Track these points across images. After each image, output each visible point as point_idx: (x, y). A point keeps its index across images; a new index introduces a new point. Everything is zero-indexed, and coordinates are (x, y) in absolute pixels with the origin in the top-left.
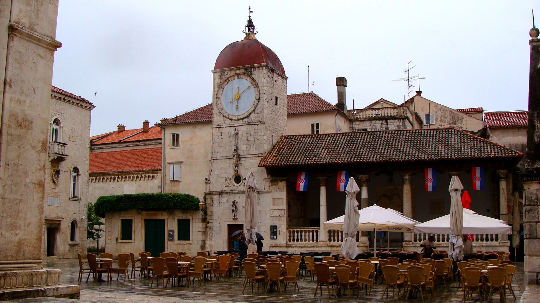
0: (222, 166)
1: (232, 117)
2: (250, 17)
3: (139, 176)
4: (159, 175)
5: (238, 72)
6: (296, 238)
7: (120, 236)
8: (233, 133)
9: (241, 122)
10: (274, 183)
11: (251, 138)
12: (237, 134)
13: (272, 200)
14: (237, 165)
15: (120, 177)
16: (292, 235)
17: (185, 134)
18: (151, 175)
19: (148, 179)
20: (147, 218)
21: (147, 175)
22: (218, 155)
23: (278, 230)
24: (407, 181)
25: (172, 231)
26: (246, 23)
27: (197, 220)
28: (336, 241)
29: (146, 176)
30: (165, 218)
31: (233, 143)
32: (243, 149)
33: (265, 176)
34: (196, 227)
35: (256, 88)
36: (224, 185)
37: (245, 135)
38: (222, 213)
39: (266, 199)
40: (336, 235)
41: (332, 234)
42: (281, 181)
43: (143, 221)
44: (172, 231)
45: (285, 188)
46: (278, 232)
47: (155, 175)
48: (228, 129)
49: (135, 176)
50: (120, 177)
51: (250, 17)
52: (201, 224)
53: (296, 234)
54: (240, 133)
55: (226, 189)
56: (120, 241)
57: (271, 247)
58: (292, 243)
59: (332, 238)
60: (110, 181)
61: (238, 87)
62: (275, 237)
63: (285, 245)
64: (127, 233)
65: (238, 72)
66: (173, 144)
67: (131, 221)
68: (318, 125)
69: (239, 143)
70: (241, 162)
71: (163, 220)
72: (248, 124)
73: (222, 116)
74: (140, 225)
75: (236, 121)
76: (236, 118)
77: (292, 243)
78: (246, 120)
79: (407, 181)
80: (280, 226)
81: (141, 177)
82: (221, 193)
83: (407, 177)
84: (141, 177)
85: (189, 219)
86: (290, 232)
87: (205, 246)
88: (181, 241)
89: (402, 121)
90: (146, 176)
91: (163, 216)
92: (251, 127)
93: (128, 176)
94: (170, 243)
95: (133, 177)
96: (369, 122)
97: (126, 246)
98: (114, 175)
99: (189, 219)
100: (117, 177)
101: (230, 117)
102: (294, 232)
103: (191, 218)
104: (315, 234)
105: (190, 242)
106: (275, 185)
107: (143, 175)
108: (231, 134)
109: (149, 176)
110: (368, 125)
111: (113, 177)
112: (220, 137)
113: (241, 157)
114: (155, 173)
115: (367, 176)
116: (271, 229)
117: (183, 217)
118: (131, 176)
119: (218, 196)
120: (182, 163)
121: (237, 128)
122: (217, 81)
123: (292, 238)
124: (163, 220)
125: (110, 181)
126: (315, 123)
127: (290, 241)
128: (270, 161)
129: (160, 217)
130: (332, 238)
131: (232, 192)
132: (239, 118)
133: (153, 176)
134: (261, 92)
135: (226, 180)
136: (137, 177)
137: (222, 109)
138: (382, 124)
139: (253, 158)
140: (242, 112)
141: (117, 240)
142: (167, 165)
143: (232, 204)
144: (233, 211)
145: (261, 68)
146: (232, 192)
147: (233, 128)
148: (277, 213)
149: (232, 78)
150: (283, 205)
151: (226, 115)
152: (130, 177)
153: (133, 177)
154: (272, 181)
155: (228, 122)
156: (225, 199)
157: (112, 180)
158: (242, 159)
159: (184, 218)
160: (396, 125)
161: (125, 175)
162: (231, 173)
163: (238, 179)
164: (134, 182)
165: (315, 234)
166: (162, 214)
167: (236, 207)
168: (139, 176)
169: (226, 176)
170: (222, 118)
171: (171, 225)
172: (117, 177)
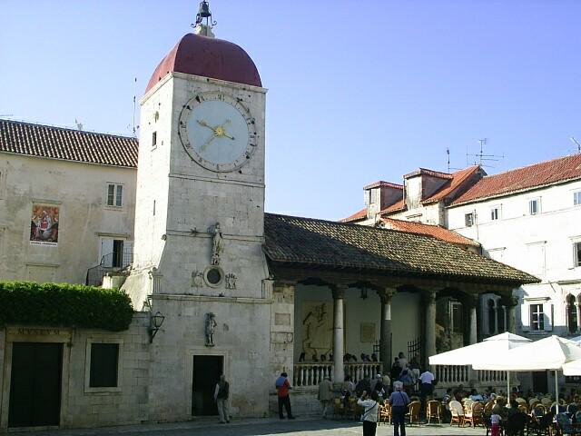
0: (186, 249)
10: (277, 289)
11: (242, 209)
16: (297, 374)
20: (21, 339)
24: (433, 301)
26: (198, 9)
30: (66, 340)
32: (228, 224)
33: (265, 272)
36: (190, 283)
38: (185, 336)
39: (265, 313)
42: (289, 286)
52: (140, 355)
54: (222, 195)
55: (193, 291)
57: (271, 394)
76: (214, 168)
77: (297, 387)
78: (234, 175)
79: (433, 301)
85: (117, 346)
87: (147, 396)
88: (100, 389)
91: (62, 337)
99: (117, 346)
102: (300, 368)
103: (121, 342)
106: (279, 291)
119: (176, 304)
122: (183, 96)
123: (297, 379)
124: (59, 347)
128: (281, 254)
129: (52, 338)
135: (194, 275)
137: (188, 146)
139: (245, 243)
143: (202, 318)
148: (281, 338)
151: (197, 159)
154: (274, 285)
155: (200, 171)
156: (189, 310)
162: (204, 266)
163: (215, 276)
166: (57, 333)
169: (194, 267)
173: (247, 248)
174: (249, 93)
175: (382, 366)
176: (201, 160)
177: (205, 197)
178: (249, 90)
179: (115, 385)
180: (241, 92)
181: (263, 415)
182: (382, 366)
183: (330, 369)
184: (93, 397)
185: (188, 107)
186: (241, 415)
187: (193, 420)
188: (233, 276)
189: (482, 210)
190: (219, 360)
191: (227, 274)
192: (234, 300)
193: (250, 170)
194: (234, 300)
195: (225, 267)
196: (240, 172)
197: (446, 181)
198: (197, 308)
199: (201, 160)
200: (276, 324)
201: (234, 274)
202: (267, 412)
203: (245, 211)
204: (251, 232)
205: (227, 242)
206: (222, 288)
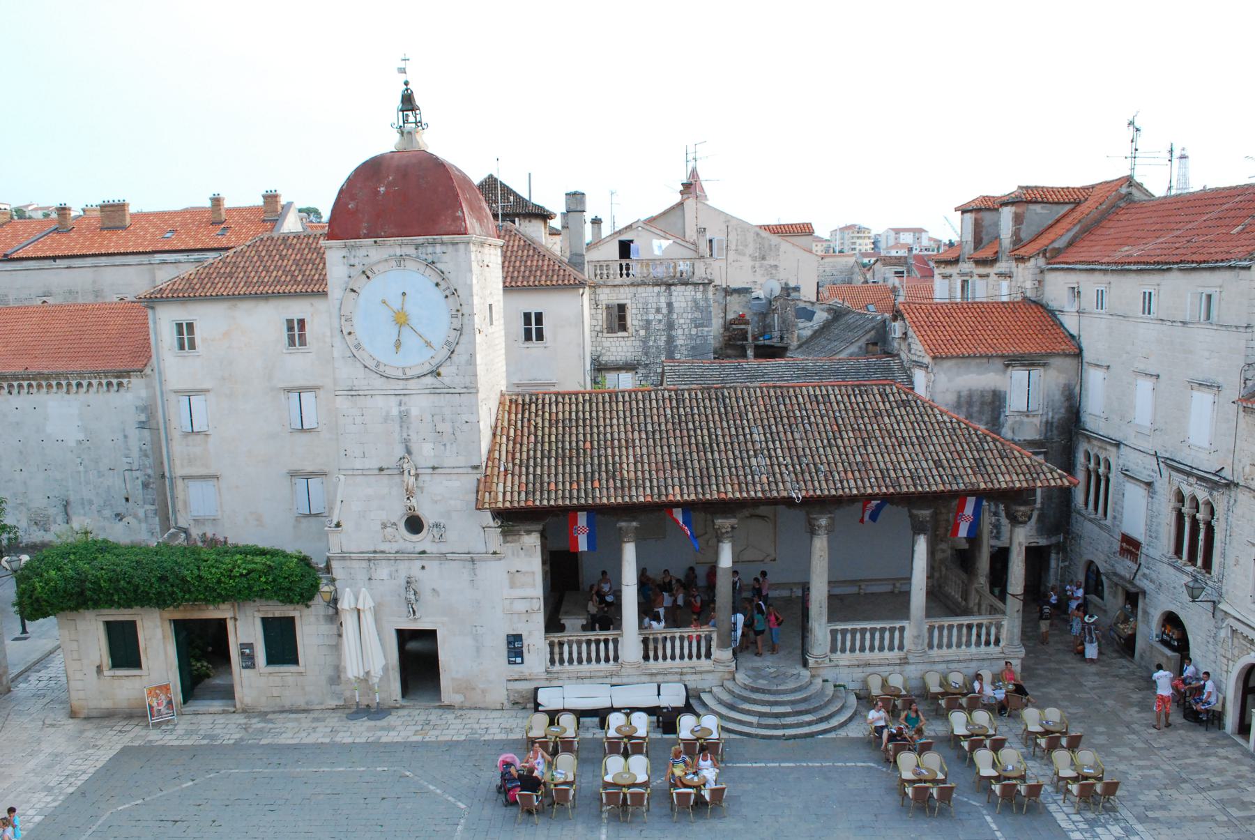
1: (389, 372)
2: (406, 83)
3: (85, 383)
4: (133, 380)
5: (398, 251)
6: (566, 656)
7: (107, 661)
8: (395, 411)
9: (412, 384)
10: (509, 538)
11: (445, 427)
12: (404, 417)
13: (505, 575)
14: (410, 494)
15: (34, 383)
17: (209, 320)
18: (115, 381)
19: (108, 390)
20: (179, 615)
21: (104, 382)
22: (358, 464)
23: (526, 643)
25: (250, 646)
27: (313, 619)
28: (660, 659)
29: (100, 384)
31: (396, 436)
32: (426, 452)
34: (310, 630)
35: (451, 299)
37: (428, 418)
39: (493, 573)
40: (660, 647)
41: (651, 646)
42: (529, 532)
43: (170, 631)
44: (250, 646)
45: (539, 548)
46: (525, 650)
47: (125, 381)
48: (380, 402)
49: (74, 383)
50: (34, 383)
51: (406, 83)
53: (566, 648)
54: (414, 412)
56: (107, 673)
58: (557, 667)
59: (651, 654)
60: (10, 393)
61: (404, 294)
62: (519, 660)
63: (544, 676)
64: (124, 650)
65: (398, 251)
66: (182, 347)
67: (131, 627)
68: (539, 317)
69: (414, 437)
70: (421, 484)
71: (222, 624)
72: (434, 391)
73: (358, 365)
74: (159, 633)
75: (401, 382)
76: (399, 374)
77: (557, 667)
78: (429, 380)
80: (530, 633)
81: (90, 384)
82: (373, 557)
83: (823, 522)
84: (90, 384)
85: (292, 619)
86: (551, 645)
87: (339, 677)
89: (701, 288)
90: (100, 384)
92: (442, 400)
93: (54, 383)
94: (246, 672)
95: (69, 385)
96: (633, 289)
97: (127, 684)
98: (17, 379)
100: (25, 383)
101: (382, 368)
103: (296, 614)
104: (611, 646)
105: (301, 668)
107: (95, 382)
108: (388, 413)
109: (109, 384)
110: (629, 296)
111: (15, 384)
112: (358, 420)
113: (420, 471)
114: (124, 377)
115: (733, 521)
116: (509, 643)
117: (278, 610)
118: (64, 383)
119: (364, 564)
120: (208, 391)
121: (404, 399)
123: (557, 657)
124: (222, 624)
125: (10, 393)
126: (533, 310)
127: (552, 662)
129: (212, 613)
130: (651, 654)
131: (399, 556)
132: (409, 373)
133: (120, 384)
134: (465, 310)
135: (384, 526)
136: (79, 385)
137: (358, 347)
138: (658, 294)
139: (454, 477)
140: (416, 358)
141: (99, 669)
142: (173, 397)
143: (403, 583)
144: (409, 603)
145: (462, 247)
146: (399, 556)
147: (393, 401)
148: (521, 606)
149: (381, 267)
150: (534, 586)
151: (371, 364)
152: (59, 385)
153: (69, 385)
154: (505, 534)
155: (379, 382)
156: (383, 571)
157: (15, 391)
158: (421, 478)
159: (277, 614)
160: (689, 298)
161: (47, 379)
163: (415, 524)
164: (72, 396)
165: (611, 646)
167: (415, 594)
168: (85, 383)
169: (383, 516)
170: (361, 372)
171: (246, 630)
172: (25, 383)
173: (457, 484)
174: (444, 248)
175: (714, 636)
176: (378, 365)
177: (387, 418)
178: (442, 243)
179: (295, 661)
180: (430, 249)
181: (499, 706)
182: (714, 636)
183: (616, 642)
184: (271, 678)
185: (353, 290)
186: (467, 704)
187: (403, 707)
188: (437, 525)
189: (1090, 284)
190: (431, 635)
191: (431, 521)
192: (443, 557)
193: (453, 369)
194: (443, 557)
195: (428, 515)
196: (439, 374)
197: (1068, 208)
198: (393, 569)
199: (378, 365)
200: (512, 588)
201: (442, 521)
202: (505, 702)
203: (451, 431)
204: (461, 461)
205: (427, 478)
206: (422, 541)
